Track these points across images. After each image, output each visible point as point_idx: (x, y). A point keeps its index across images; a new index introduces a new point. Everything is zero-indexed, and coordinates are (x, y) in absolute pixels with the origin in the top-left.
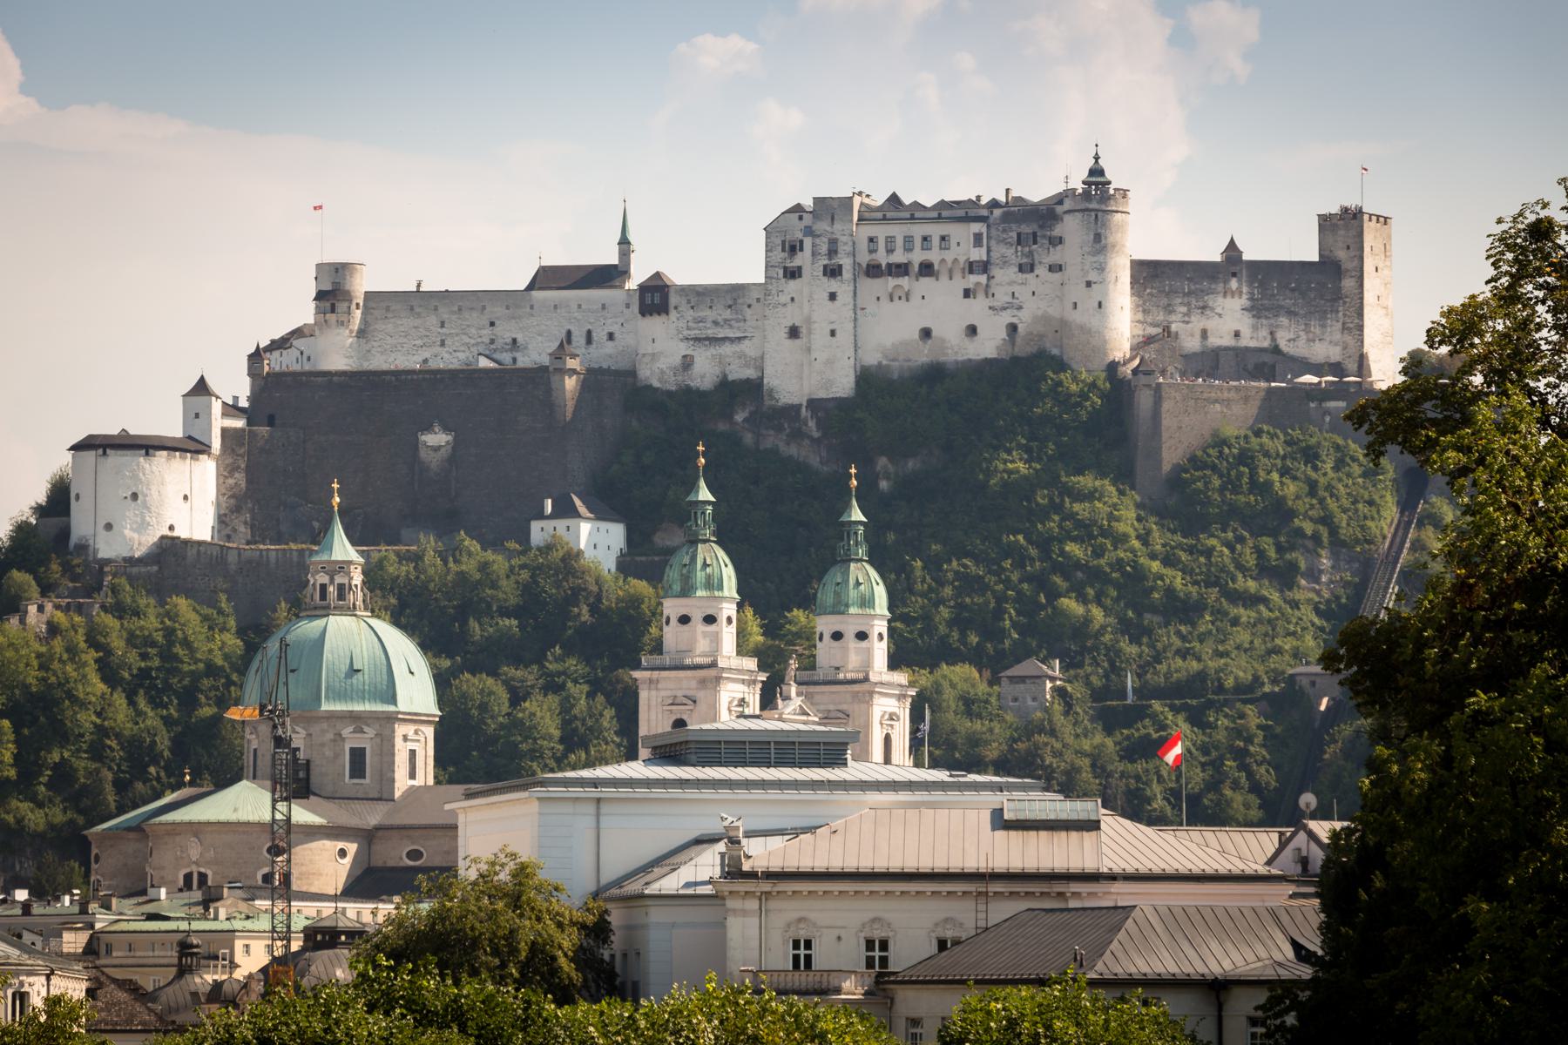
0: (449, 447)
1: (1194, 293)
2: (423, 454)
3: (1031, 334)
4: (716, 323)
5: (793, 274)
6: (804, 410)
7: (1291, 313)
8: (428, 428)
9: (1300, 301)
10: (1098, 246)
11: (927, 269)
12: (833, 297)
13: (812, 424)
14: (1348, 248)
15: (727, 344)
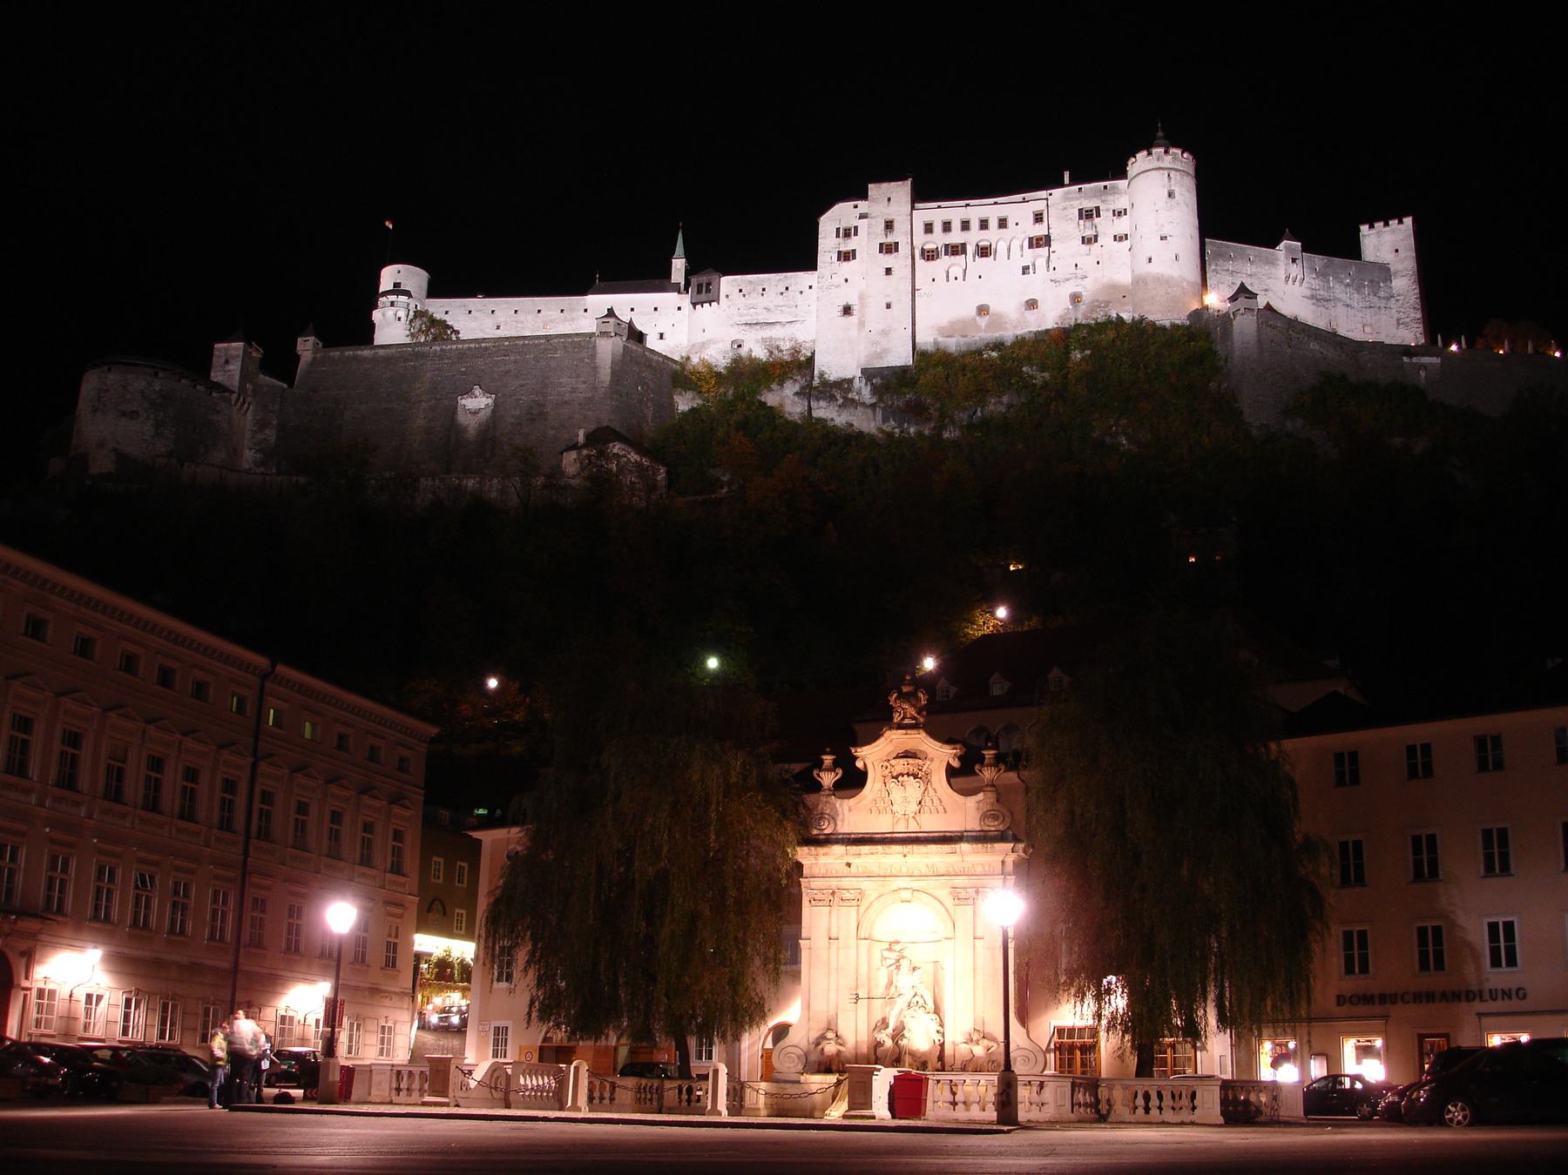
0: (489, 411)
1: (1255, 275)
2: (462, 418)
3: (1097, 301)
4: (767, 309)
5: (846, 256)
6: (857, 384)
7: (1347, 306)
8: (468, 392)
9: (1356, 295)
10: (1172, 202)
11: (984, 252)
12: (888, 271)
13: (866, 395)
14: (1397, 251)
15: (778, 327)
